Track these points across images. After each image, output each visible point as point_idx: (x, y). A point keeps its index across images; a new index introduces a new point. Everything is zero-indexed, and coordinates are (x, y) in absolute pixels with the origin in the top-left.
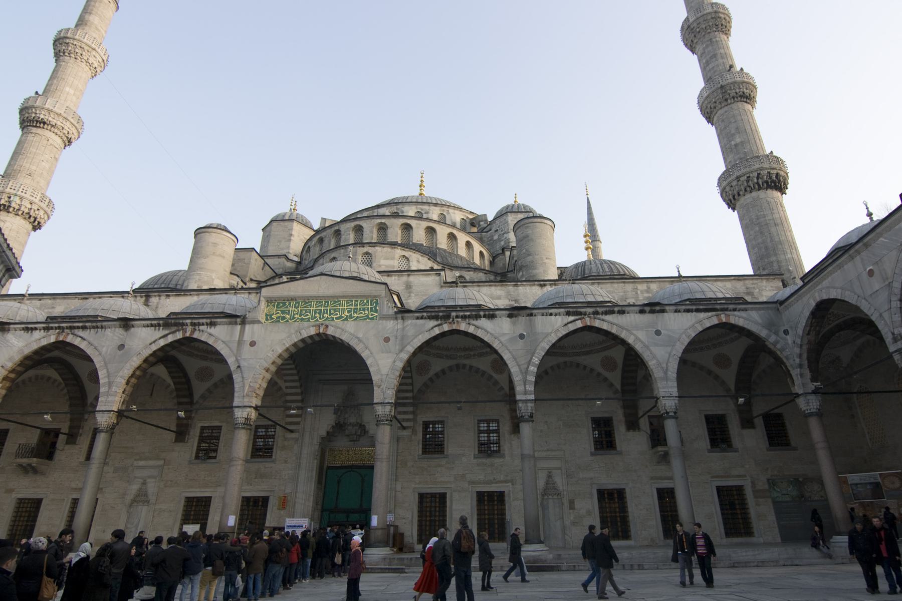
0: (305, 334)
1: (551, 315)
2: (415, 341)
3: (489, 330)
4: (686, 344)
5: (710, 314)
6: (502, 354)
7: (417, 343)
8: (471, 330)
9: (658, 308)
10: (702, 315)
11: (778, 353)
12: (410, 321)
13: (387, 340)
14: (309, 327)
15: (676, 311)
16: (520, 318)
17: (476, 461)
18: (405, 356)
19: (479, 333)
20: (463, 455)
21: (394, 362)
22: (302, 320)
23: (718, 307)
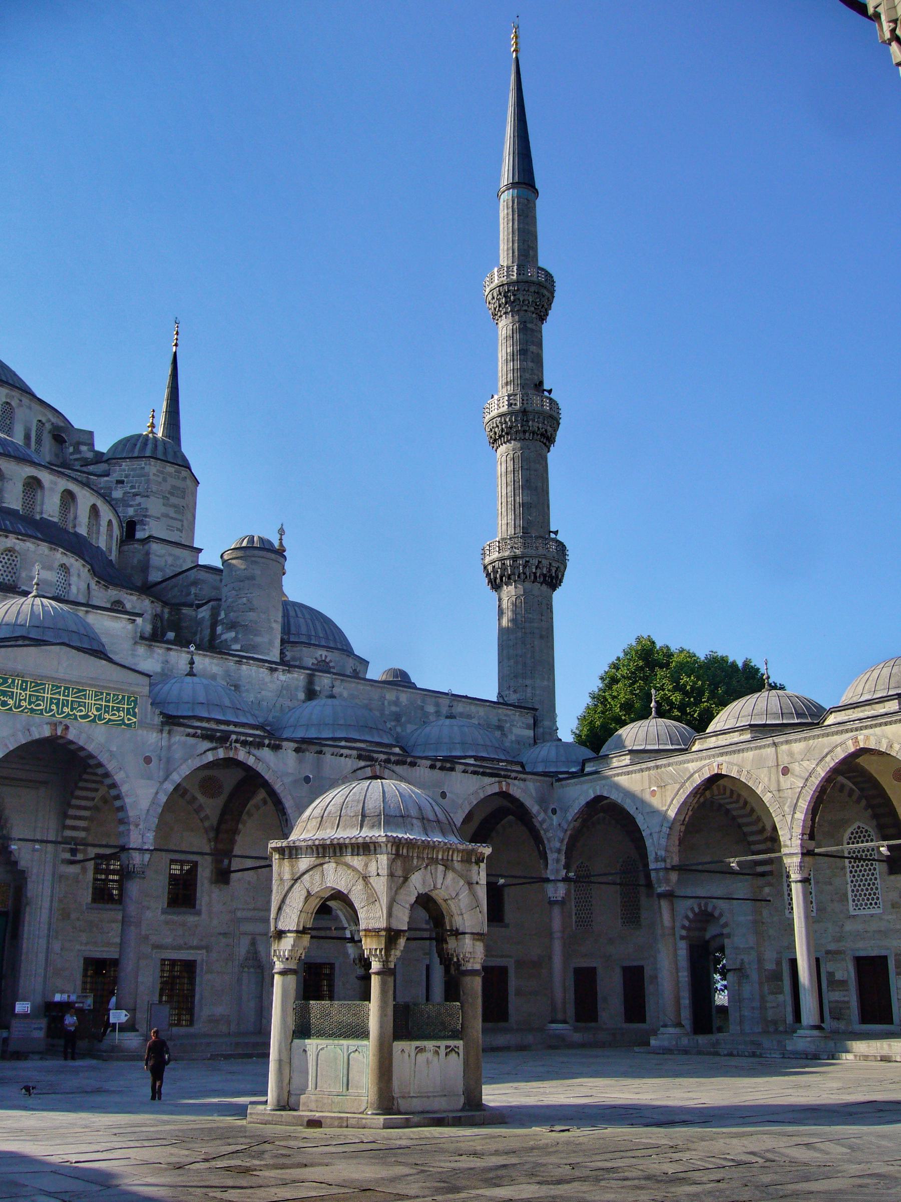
0: (36, 736)
1: (341, 755)
2: (184, 766)
3: (272, 765)
4: (467, 812)
5: (493, 779)
6: (284, 800)
7: (185, 770)
8: (251, 761)
9: (448, 765)
10: (487, 780)
11: (542, 832)
12: (177, 738)
13: (148, 760)
14: (40, 725)
15: (464, 772)
16: (307, 753)
17: (163, 917)
18: (169, 787)
19: (260, 768)
20: (148, 908)
21: (157, 793)
22: (32, 710)
23: (502, 773)
